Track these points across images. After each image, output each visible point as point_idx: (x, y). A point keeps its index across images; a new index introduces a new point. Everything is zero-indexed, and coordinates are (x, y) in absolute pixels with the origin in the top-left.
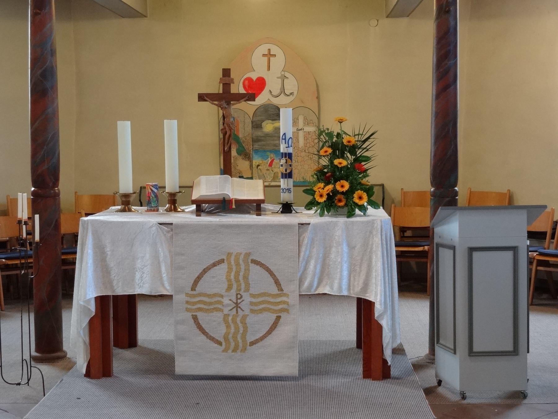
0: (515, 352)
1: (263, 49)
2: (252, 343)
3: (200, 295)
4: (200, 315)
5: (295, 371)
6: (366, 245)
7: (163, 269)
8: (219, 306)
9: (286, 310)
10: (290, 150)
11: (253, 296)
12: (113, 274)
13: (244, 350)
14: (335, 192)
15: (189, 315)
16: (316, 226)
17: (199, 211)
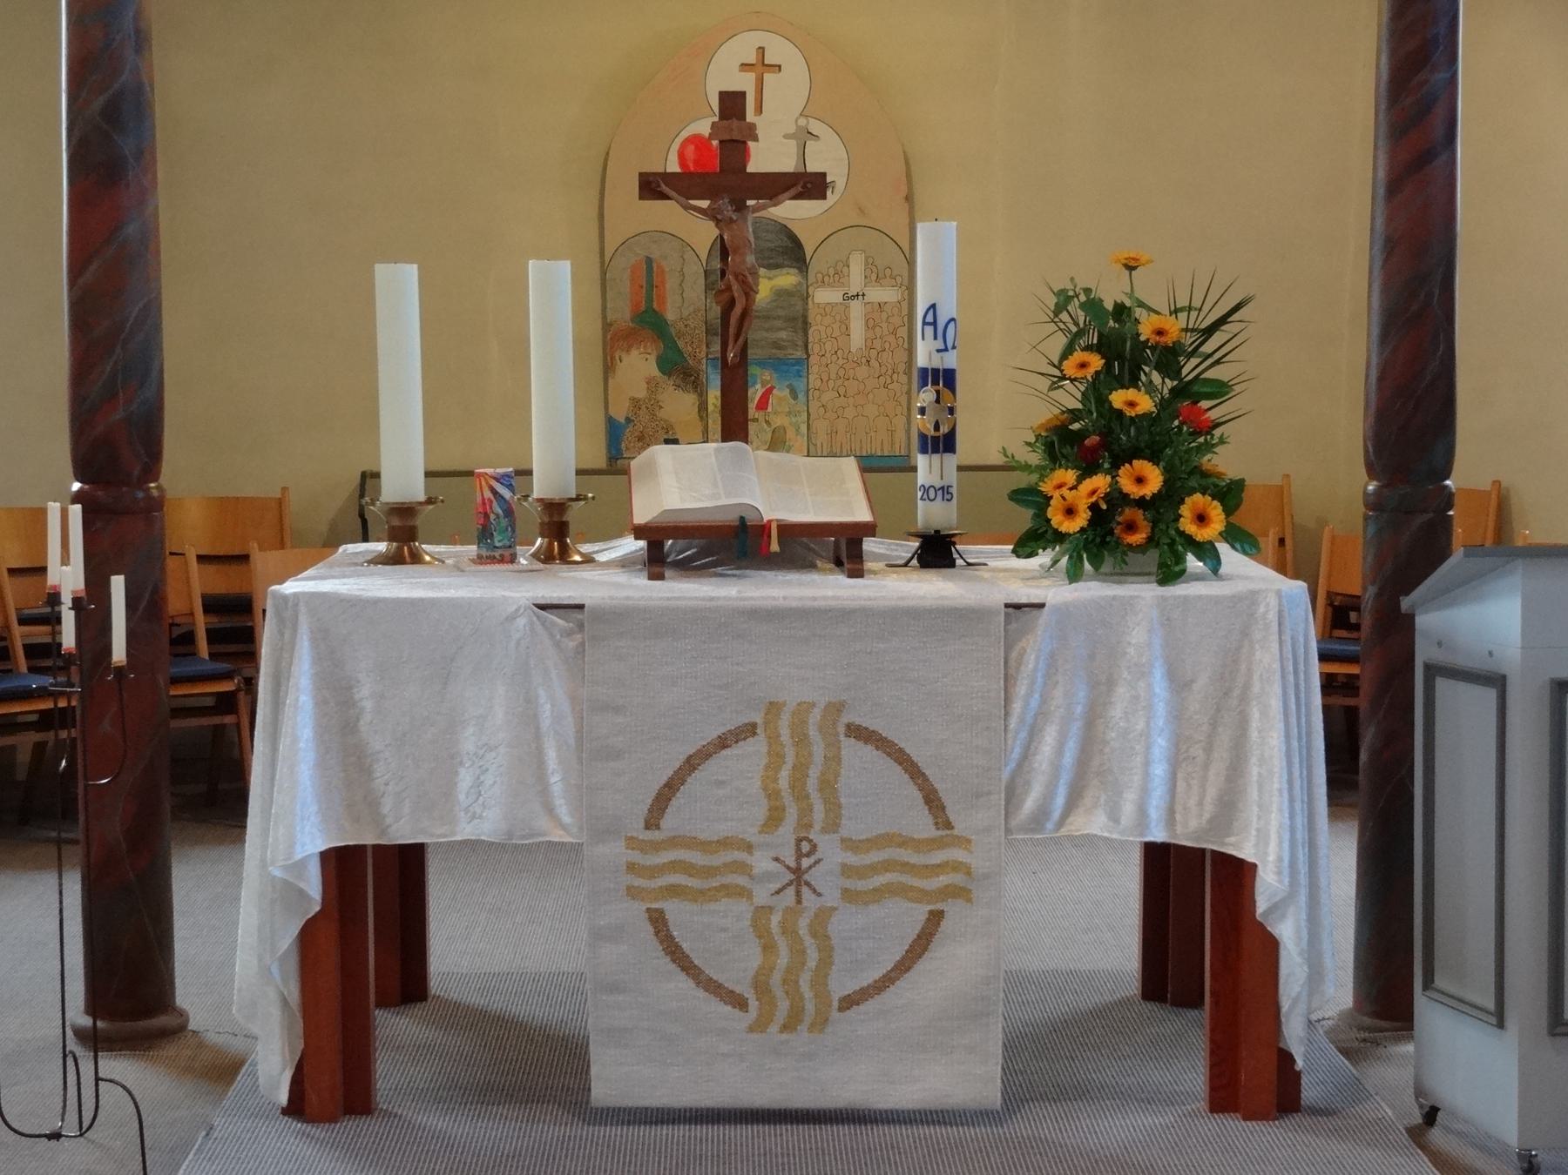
1: (742, 47)
2: (849, 1002)
3: (675, 842)
4: (674, 910)
7: (551, 755)
8: (742, 881)
9: (959, 893)
10: (950, 360)
11: (850, 845)
12: (383, 772)
13: (821, 1023)
14: (1117, 499)
15: (639, 908)
16: (1065, 612)
17: (656, 562)
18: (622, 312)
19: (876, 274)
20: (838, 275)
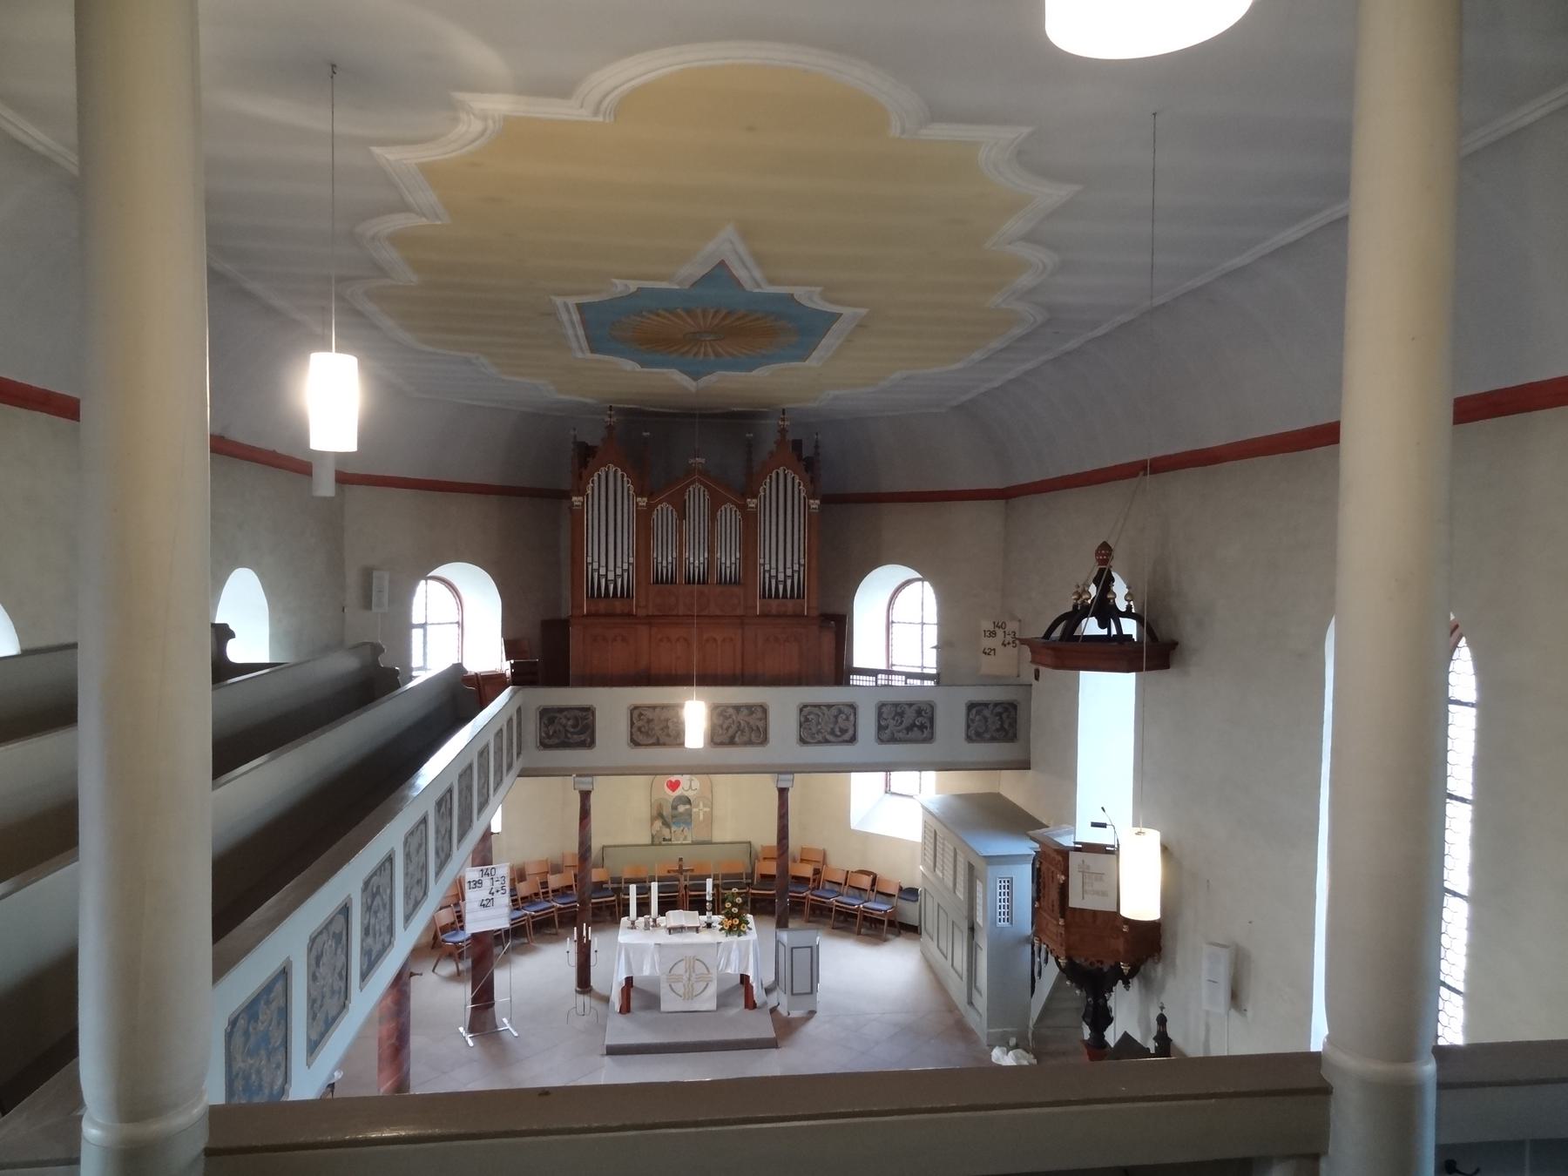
0: (811, 993)
4: (673, 985)
5: (715, 1008)
6: (747, 948)
18: (655, 813)
19: (705, 806)
20: (698, 806)
